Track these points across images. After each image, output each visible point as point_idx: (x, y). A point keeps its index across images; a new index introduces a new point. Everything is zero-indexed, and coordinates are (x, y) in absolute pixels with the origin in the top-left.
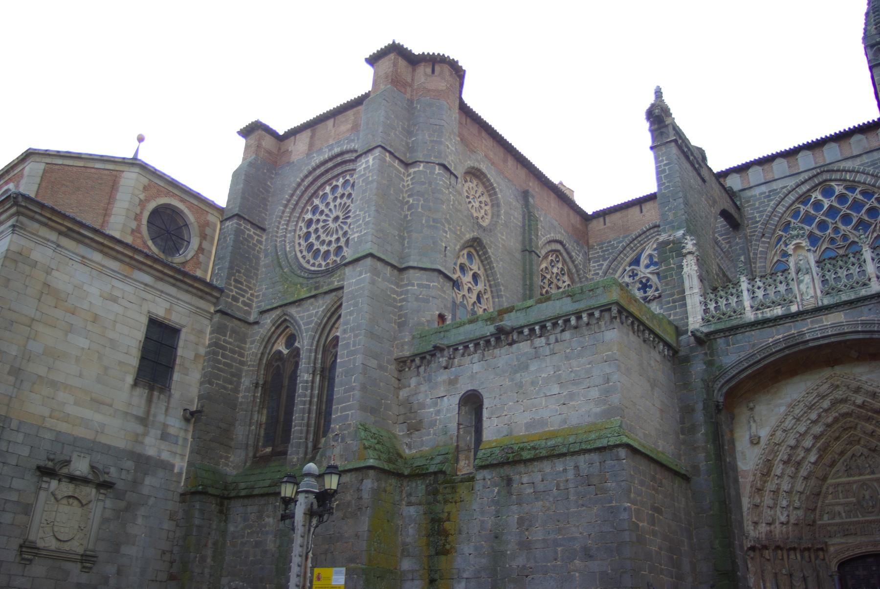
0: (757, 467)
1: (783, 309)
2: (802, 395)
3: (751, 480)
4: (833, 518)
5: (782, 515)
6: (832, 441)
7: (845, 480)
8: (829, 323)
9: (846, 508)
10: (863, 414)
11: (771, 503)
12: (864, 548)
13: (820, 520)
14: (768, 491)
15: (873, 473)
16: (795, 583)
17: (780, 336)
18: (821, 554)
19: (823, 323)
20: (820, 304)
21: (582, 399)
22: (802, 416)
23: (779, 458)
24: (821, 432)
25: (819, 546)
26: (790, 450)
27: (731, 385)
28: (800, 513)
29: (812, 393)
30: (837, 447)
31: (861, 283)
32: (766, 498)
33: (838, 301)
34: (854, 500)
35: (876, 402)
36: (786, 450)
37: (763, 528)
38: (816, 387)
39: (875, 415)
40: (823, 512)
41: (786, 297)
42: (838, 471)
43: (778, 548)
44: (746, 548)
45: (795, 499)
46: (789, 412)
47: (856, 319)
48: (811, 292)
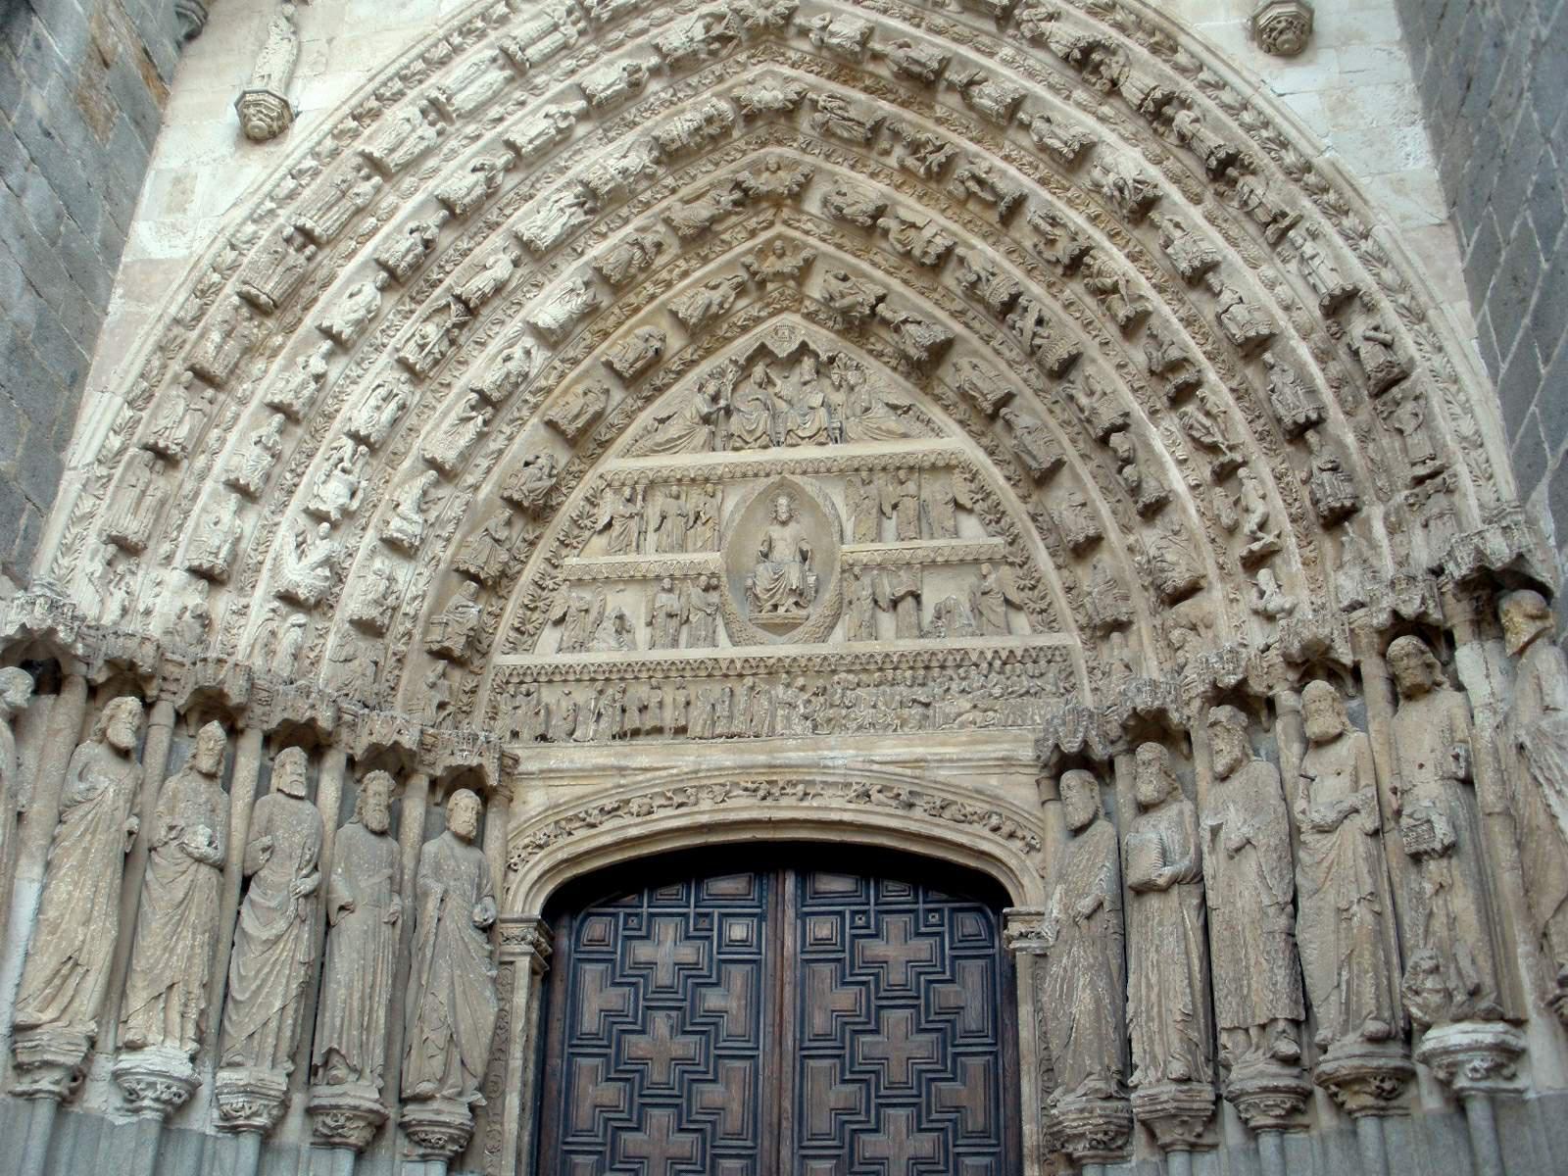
0: (230, 256)
3: (173, 310)
4: (581, 646)
6: (673, 248)
7: (688, 461)
9: (664, 598)
10: (852, 114)
12: (706, 804)
13: (515, 648)
14: (254, 403)
15: (840, 436)
16: (248, 922)
18: (465, 801)
22: (547, 57)
23: (366, 251)
24: (624, 172)
25: (467, 758)
26: (443, 225)
28: (411, 580)
32: (232, 437)
34: (713, 559)
35: (930, 30)
39: (908, 115)
40: (536, 615)
42: (662, 421)
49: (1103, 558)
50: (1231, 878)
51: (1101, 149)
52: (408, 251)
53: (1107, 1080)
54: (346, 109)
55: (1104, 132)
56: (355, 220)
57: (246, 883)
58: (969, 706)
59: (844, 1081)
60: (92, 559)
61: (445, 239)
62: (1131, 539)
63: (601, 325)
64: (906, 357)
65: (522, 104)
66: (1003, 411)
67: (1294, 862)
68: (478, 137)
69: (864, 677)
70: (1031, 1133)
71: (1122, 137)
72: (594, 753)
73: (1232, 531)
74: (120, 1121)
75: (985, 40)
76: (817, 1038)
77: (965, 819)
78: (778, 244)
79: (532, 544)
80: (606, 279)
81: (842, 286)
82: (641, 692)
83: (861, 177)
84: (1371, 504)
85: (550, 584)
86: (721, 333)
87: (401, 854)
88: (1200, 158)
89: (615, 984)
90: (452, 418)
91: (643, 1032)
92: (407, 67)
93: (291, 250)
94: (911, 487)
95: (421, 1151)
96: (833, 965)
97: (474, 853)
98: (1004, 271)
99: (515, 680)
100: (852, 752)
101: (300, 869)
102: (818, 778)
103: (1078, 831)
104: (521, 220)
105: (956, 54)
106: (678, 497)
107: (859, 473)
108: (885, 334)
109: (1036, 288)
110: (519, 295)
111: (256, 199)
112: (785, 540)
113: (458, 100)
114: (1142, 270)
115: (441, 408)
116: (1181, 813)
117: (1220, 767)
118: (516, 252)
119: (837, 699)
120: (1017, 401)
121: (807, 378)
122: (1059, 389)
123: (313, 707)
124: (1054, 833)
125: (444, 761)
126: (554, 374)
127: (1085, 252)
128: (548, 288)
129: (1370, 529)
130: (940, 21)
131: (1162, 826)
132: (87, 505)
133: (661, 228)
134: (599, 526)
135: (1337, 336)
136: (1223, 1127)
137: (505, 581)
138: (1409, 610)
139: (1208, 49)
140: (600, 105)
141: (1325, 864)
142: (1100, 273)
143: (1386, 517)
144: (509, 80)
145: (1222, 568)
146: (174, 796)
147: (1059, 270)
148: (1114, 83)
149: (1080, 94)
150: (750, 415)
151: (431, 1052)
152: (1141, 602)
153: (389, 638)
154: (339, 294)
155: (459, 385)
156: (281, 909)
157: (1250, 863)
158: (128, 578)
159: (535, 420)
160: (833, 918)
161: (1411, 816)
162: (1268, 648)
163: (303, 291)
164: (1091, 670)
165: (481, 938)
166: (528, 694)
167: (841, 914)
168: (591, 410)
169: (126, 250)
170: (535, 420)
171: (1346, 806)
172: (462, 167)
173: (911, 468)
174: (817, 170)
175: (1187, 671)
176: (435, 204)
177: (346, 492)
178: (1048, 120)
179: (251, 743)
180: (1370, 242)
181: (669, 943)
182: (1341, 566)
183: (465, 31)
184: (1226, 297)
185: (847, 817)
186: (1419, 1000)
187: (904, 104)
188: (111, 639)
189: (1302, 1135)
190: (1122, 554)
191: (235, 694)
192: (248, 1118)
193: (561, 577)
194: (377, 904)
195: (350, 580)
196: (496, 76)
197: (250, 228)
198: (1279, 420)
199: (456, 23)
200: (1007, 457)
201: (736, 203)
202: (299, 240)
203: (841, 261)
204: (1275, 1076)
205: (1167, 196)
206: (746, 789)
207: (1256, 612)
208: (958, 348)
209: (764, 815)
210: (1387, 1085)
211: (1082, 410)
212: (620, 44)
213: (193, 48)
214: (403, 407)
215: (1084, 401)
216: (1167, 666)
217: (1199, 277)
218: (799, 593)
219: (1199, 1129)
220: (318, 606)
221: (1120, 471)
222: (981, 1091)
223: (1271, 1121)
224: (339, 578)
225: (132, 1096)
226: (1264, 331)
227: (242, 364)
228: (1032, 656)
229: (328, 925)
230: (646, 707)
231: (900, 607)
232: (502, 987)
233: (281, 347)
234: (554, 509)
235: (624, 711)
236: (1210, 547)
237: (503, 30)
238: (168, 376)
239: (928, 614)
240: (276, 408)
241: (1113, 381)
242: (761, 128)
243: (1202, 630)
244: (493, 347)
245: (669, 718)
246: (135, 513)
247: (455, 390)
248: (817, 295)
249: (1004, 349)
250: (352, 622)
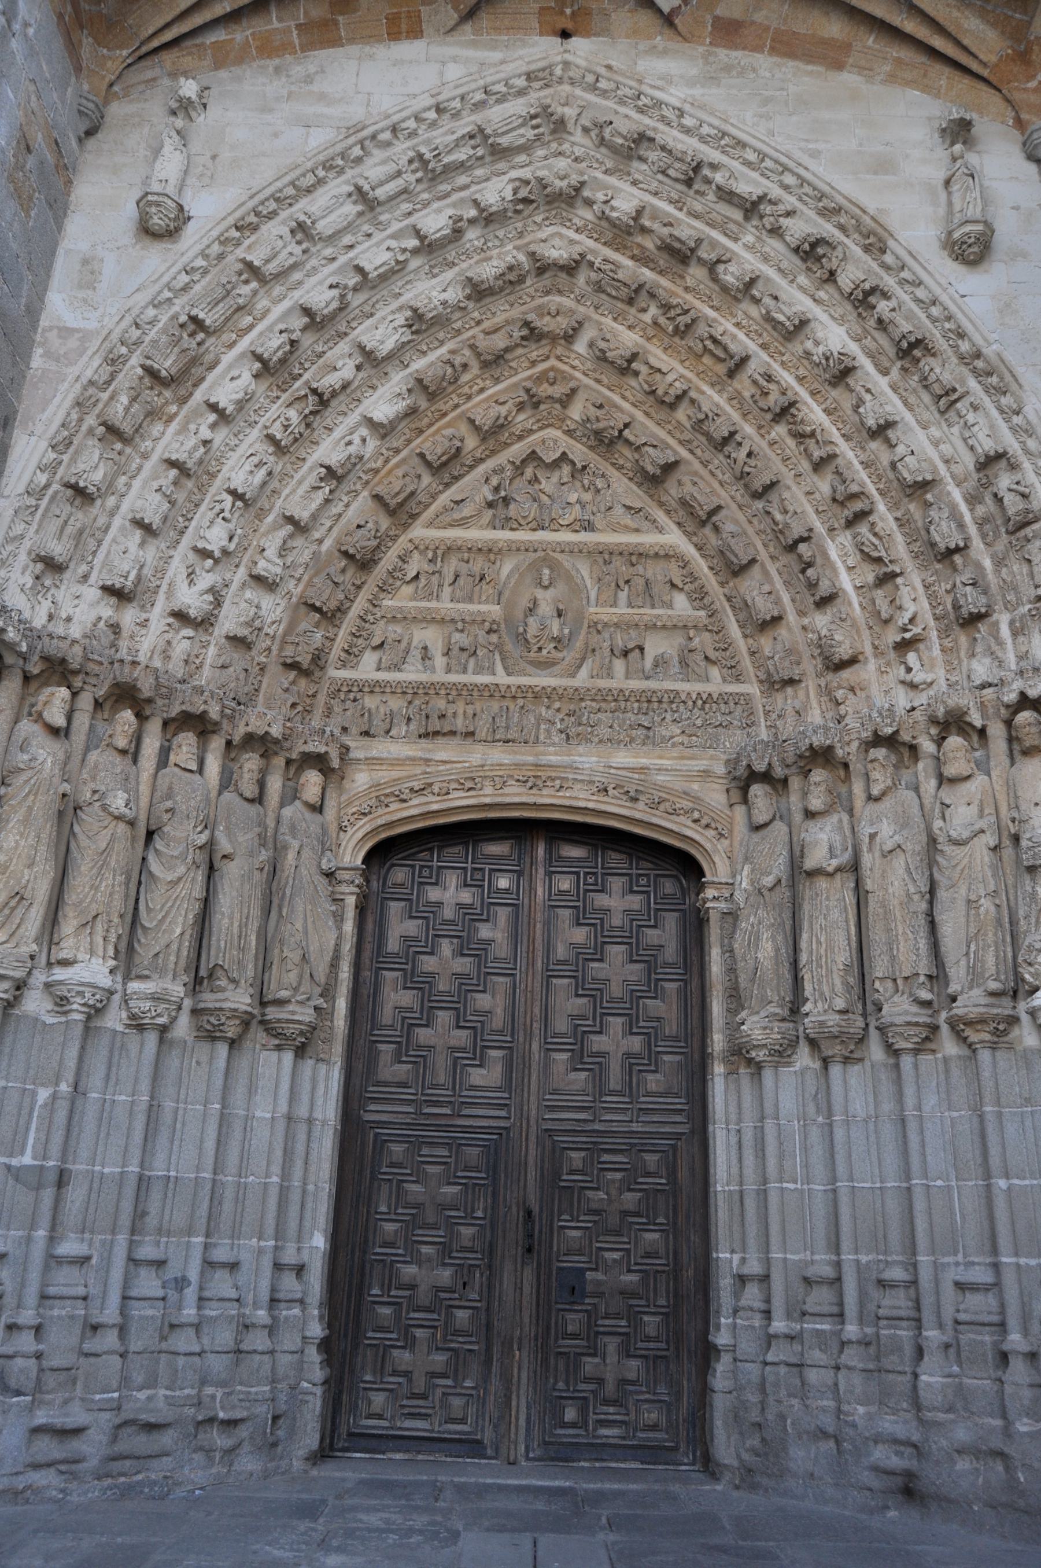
0: (135, 333)
3: (89, 373)
4: (396, 667)
5: (191, 582)
6: (475, 369)
9: (457, 636)
10: (620, 276)
11: (153, 508)
12: (488, 790)
14: (155, 458)
15: (589, 526)
16: (154, 865)
18: (312, 781)
22: (392, 198)
24: (444, 303)
26: (304, 330)
29: (456, 115)
32: (137, 483)
34: (494, 611)
36: (281, 319)
38: (479, 96)
39: (664, 282)
40: (360, 641)
42: (457, 503)
45: (264, 542)
49: (782, 632)
50: (884, 871)
51: (812, 324)
52: (279, 348)
53: (782, 1006)
54: (231, 220)
55: (817, 312)
56: (236, 317)
57: (150, 835)
58: (679, 731)
59: (577, 995)
60: (23, 573)
61: (307, 340)
62: (806, 621)
63: (418, 424)
64: (643, 471)
65: (369, 235)
66: (714, 519)
67: (932, 863)
68: (334, 259)
69: (603, 705)
70: (718, 1041)
71: (832, 317)
72: (407, 747)
73: (886, 622)
74: (50, 1020)
75: (731, 226)
76: (559, 962)
77: (675, 812)
78: (551, 374)
79: (359, 587)
80: (425, 388)
81: (599, 413)
82: (441, 704)
83: (621, 328)
84: (1000, 613)
85: (370, 618)
86: (503, 439)
87: (265, 816)
88: (892, 340)
89: (411, 917)
90: (305, 486)
91: (432, 953)
92: (281, 191)
93: (185, 335)
94: (640, 569)
95: (277, 1042)
96: (570, 911)
97: (317, 817)
98: (726, 413)
99: (344, 689)
100: (594, 759)
101: (195, 827)
102: (571, 776)
103: (758, 828)
104: (363, 333)
105: (708, 236)
106: (468, 562)
108: (627, 452)
109: (748, 429)
110: (359, 394)
111: (157, 287)
112: (547, 601)
113: (320, 226)
114: (834, 423)
115: (297, 476)
116: (840, 821)
117: (875, 791)
118: (359, 360)
119: (584, 720)
120: (723, 513)
121: (565, 480)
122: (759, 505)
123: (205, 702)
125: (300, 748)
126: (381, 459)
127: (792, 404)
128: (380, 391)
129: (998, 631)
130: (698, 207)
131: (828, 828)
132: (19, 528)
133: (467, 352)
134: (408, 578)
136: (868, 1047)
137: (338, 615)
139: (910, 253)
140: (429, 245)
141: (959, 868)
142: (802, 421)
143: (1012, 623)
144: (360, 214)
145: (876, 648)
146: (96, 767)
147: (769, 416)
148: (832, 273)
149: (802, 280)
150: (523, 507)
151: (289, 967)
152: (810, 666)
153: (254, 652)
154: (222, 376)
155: (310, 461)
156: (183, 857)
157: (899, 862)
158: (53, 591)
159: (365, 493)
160: (572, 876)
161: (1030, 839)
162: (913, 709)
163: (193, 370)
164: (767, 713)
165: (324, 881)
166: (355, 700)
167: (577, 874)
168: (408, 490)
169: (43, 317)
170: (365, 493)
171: (977, 827)
172: (321, 283)
173: (641, 554)
175: (847, 720)
176: (298, 312)
177: (226, 537)
178: (776, 298)
179: (154, 727)
180: (1021, 417)
181: (452, 889)
182: (973, 655)
183: (328, 166)
184: (901, 450)
185: (591, 805)
186: (1032, 970)
187: (661, 273)
188: (46, 640)
189: (930, 1057)
190: (797, 630)
191: (146, 687)
192: (153, 1018)
193: (379, 615)
194: (251, 854)
195: (226, 606)
196: (351, 209)
197: (151, 312)
198: (933, 545)
199: (321, 158)
200: (712, 553)
201: (523, 338)
202: (192, 327)
203: (598, 392)
204: (916, 1014)
205: (862, 367)
206: (518, 781)
207: (903, 682)
208: (682, 468)
209: (531, 800)
210: (1001, 1027)
211: (776, 523)
212: (447, 195)
213: (91, 143)
214: (270, 474)
215: (779, 517)
216: (829, 715)
218: (558, 640)
219: (852, 1047)
220: (204, 623)
221: (803, 571)
222: (674, 1006)
223: (910, 1046)
224: (218, 603)
225: (62, 1002)
226: (929, 478)
227: (145, 424)
228: (724, 699)
229: (211, 867)
230: (444, 716)
231: (631, 656)
232: (339, 918)
233: (176, 414)
234: (375, 562)
235: (427, 717)
236: (868, 632)
237: (357, 170)
238: (84, 428)
240: (172, 464)
241: (802, 504)
242: (547, 280)
243: (858, 692)
244: (337, 433)
245: (460, 724)
246: (59, 539)
247: (309, 464)
248: (577, 417)
249: (718, 473)
250: (228, 637)
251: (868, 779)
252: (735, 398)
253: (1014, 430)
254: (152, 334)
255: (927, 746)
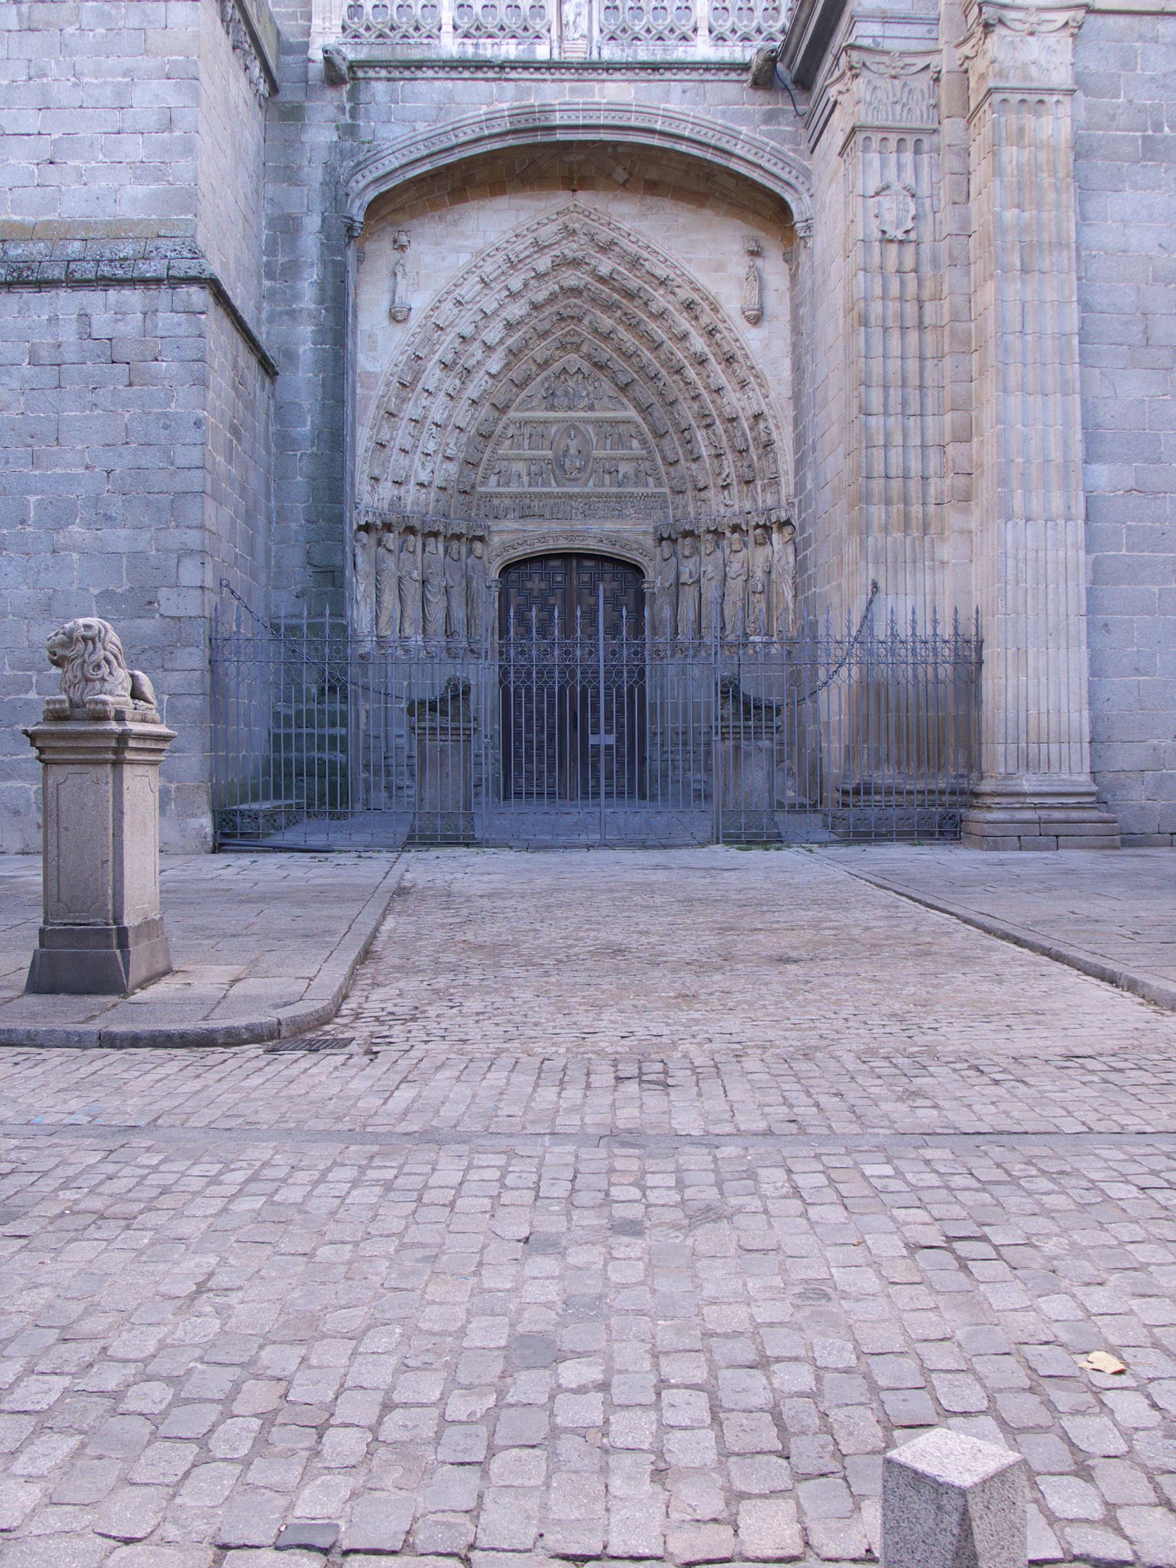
1: (521, 47)
2: (507, 237)
4: (507, 484)
8: (605, 101)
9: (533, 468)
10: (603, 296)
11: (408, 444)
12: (551, 542)
13: (483, 484)
15: (591, 408)
16: (429, 597)
17: (505, 106)
18: (478, 546)
19: (593, 96)
20: (595, 56)
21: (101, 157)
22: (495, 279)
27: (384, 188)
29: (525, 236)
30: (541, 349)
31: (678, 32)
33: (630, 60)
34: (549, 454)
36: (451, 342)
37: (386, 491)
39: (624, 301)
41: (530, 22)
43: (411, 530)
44: (355, 527)
45: (449, 441)
46: (475, 266)
47: (656, 104)
48: (583, 24)
55: (691, 330)
82: (527, 501)
107: (598, 423)
109: (663, 372)
124: (658, 558)
135: (757, 424)
138: (761, 523)
149: (685, 314)
152: (689, 486)
157: (713, 583)
174: (588, 310)
196: (479, 286)
217: (718, 391)
228: (654, 495)
239: (620, 476)
240: (411, 420)
242: (569, 294)
251: (706, 548)
252: (658, 357)
253: (767, 404)
254: (401, 366)
255: (728, 534)
